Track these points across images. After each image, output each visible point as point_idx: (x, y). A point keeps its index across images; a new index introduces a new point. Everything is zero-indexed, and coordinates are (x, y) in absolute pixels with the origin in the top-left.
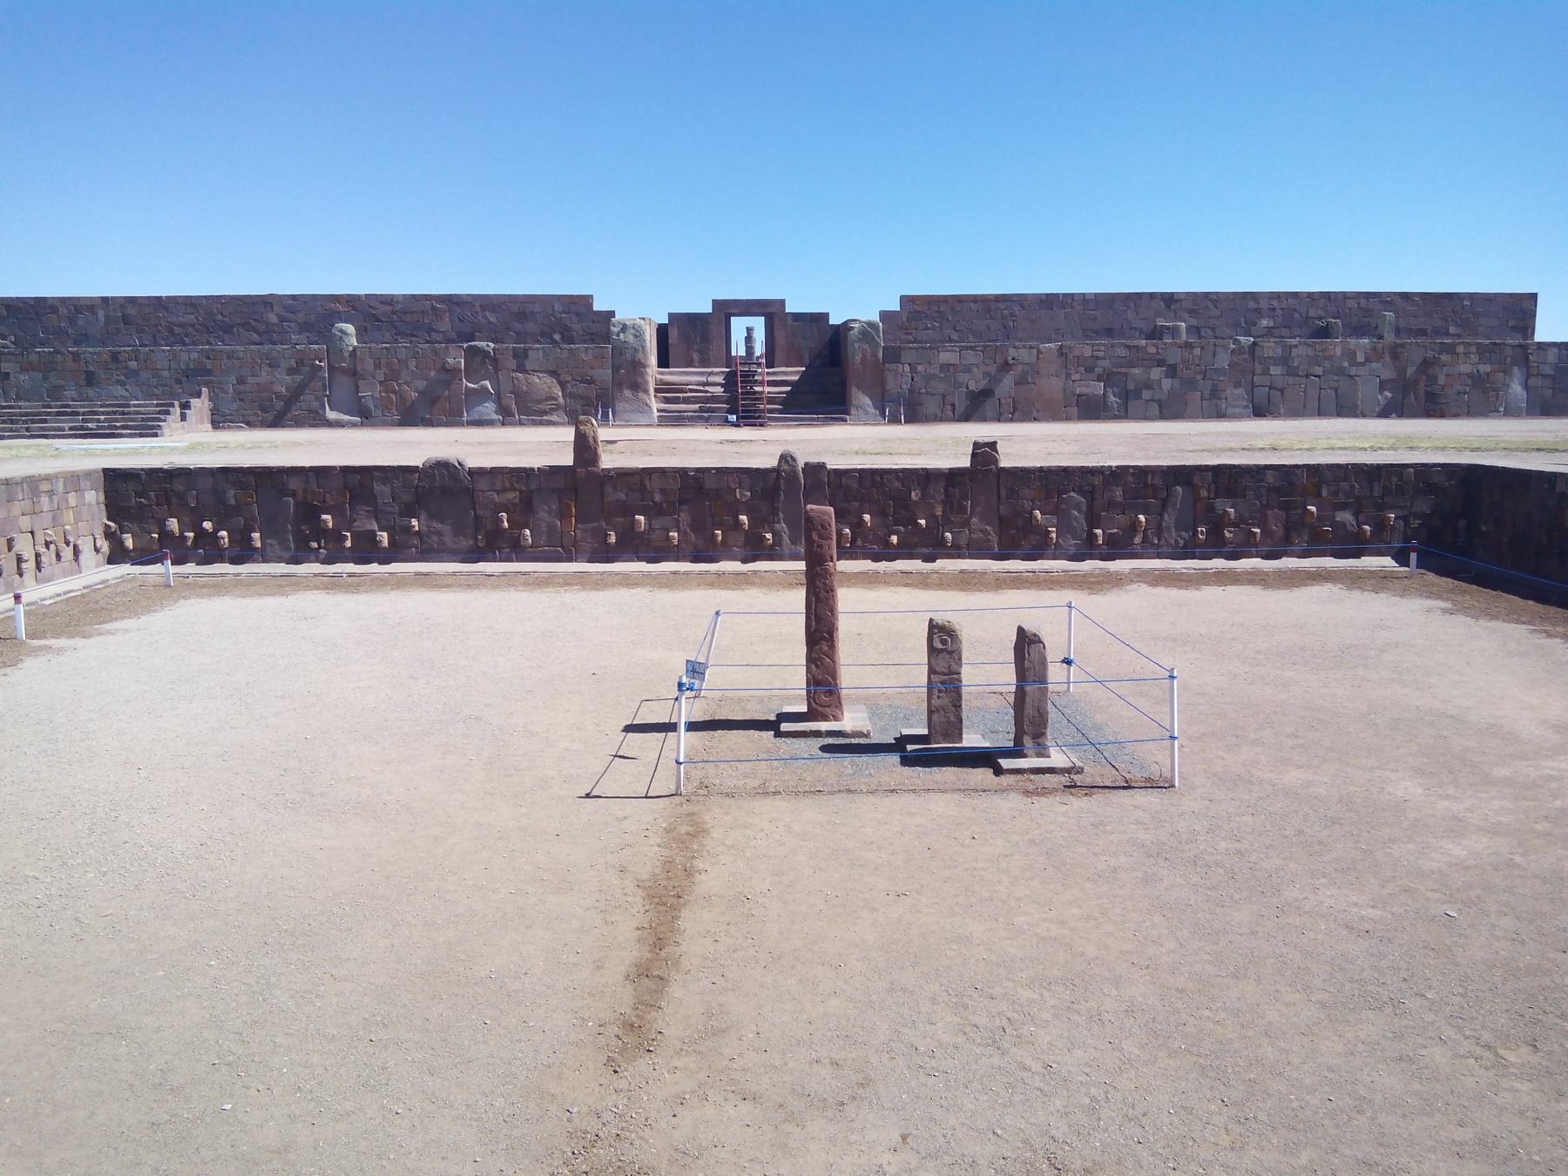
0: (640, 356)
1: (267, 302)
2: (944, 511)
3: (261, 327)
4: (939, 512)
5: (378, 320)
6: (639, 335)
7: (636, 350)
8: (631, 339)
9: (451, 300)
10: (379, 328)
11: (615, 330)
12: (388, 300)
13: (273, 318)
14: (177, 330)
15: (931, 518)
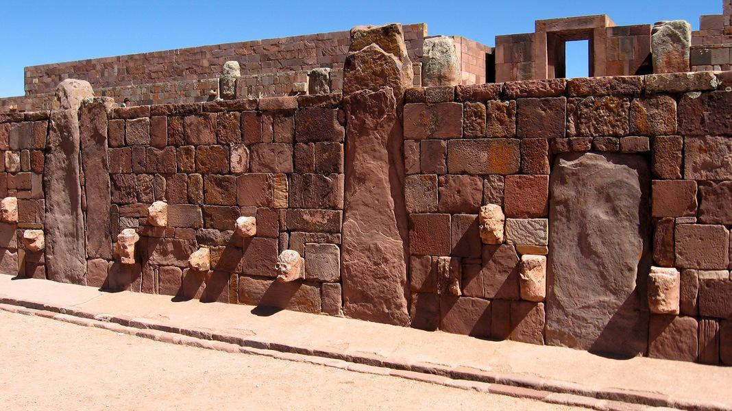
0: (444, 71)
1: (202, 51)
2: (291, 197)
3: (199, 70)
4: (281, 203)
5: (269, 59)
6: (445, 52)
7: (442, 66)
8: (438, 55)
9: (318, 39)
10: (269, 66)
11: (425, 48)
12: (276, 44)
13: (205, 63)
14: (153, 75)
15: (266, 213)
